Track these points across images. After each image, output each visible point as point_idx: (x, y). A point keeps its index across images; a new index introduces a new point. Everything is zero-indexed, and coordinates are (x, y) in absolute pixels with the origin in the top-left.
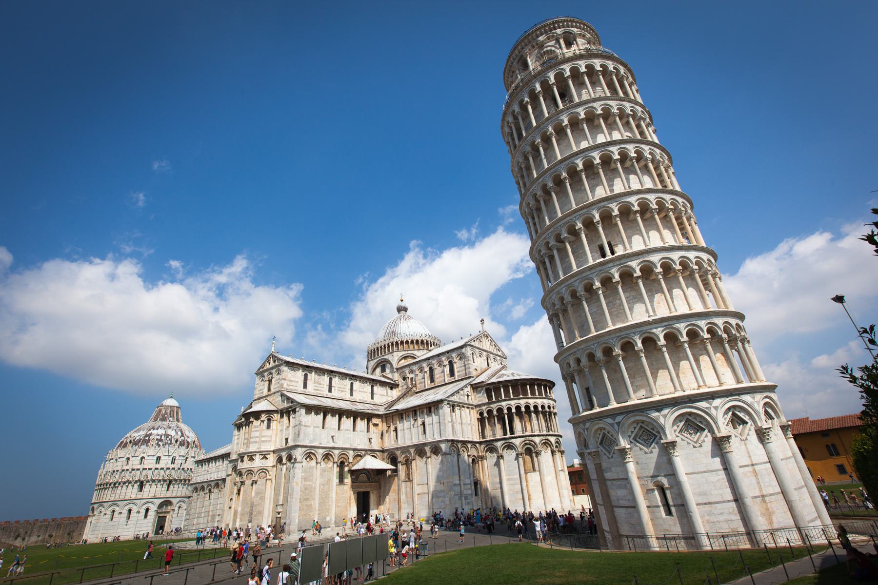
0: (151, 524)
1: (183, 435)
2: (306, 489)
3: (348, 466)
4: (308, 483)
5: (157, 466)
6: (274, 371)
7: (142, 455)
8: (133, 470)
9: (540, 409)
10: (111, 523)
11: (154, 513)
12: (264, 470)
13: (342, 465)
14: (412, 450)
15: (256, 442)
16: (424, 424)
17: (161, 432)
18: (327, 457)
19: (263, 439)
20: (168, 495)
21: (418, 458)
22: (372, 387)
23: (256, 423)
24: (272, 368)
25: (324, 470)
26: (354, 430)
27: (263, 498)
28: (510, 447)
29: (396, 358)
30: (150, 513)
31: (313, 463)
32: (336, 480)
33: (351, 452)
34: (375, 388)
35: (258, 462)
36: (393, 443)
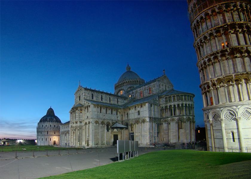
2: (96, 132)
13: (108, 126)
15: (77, 117)
16: (139, 112)
18: (103, 123)
21: (136, 123)
26: (112, 114)
28: (173, 120)
31: (98, 124)
32: (106, 130)
35: (79, 124)
36: (126, 119)
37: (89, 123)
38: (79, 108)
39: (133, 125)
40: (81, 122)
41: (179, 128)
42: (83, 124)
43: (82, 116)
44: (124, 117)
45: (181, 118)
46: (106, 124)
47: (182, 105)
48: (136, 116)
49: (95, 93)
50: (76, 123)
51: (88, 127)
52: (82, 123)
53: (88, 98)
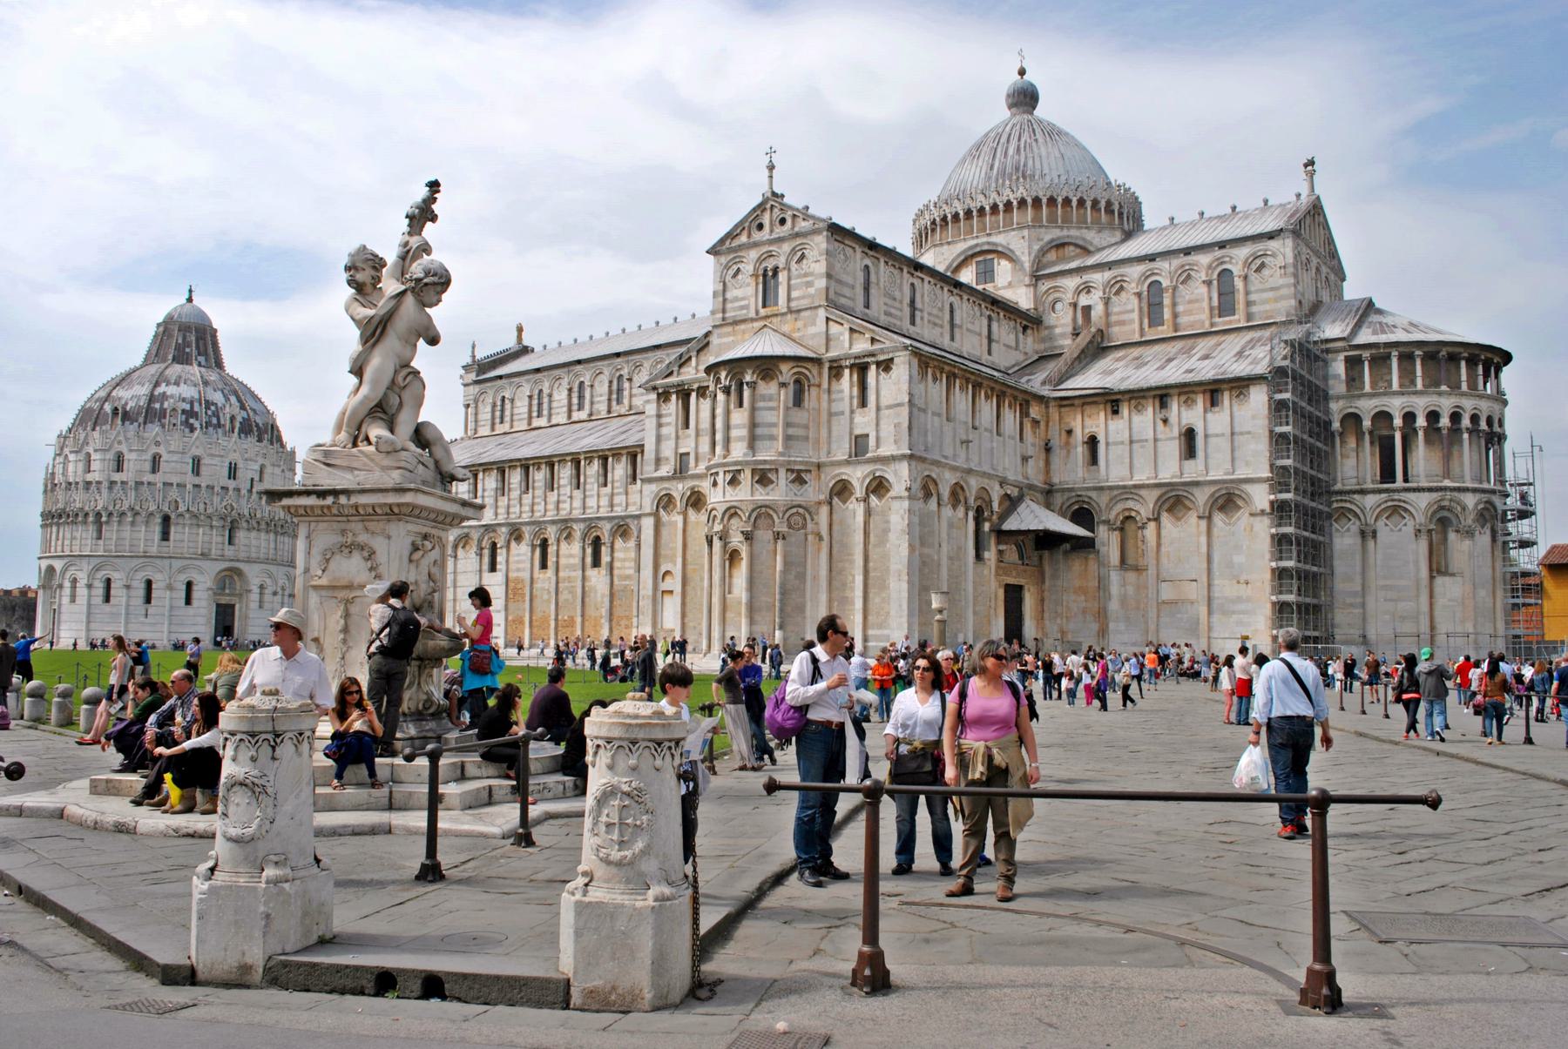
0: (201, 620)
1: (243, 407)
2: (924, 563)
3: (989, 520)
5: (197, 480)
6: (786, 247)
7: (154, 450)
8: (139, 484)
9: (1483, 425)
10: (107, 608)
11: (205, 595)
12: (799, 515)
14: (1151, 497)
15: (772, 438)
16: (1189, 435)
17: (188, 391)
19: (791, 431)
22: (990, 318)
23: (768, 388)
24: (780, 240)
25: (951, 525)
26: (998, 434)
27: (802, 577)
28: (1396, 511)
29: (1036, 247)
30: (196, 595)
32: (971, 552)
33: (997, 487)
34: (995, 325)
35: (780, 492)
37: (879, 486)
38: (784, 367)
39: (1143, 527)
41: (1438, 567)
42: (814, 492)
43: (806, 427)
44: (1056, 460)
45: (1446, 503)
47: (1455, 417)
48: (1171, 468)
50: (763, 477)
51: (860, 518)
52: (802, 482)
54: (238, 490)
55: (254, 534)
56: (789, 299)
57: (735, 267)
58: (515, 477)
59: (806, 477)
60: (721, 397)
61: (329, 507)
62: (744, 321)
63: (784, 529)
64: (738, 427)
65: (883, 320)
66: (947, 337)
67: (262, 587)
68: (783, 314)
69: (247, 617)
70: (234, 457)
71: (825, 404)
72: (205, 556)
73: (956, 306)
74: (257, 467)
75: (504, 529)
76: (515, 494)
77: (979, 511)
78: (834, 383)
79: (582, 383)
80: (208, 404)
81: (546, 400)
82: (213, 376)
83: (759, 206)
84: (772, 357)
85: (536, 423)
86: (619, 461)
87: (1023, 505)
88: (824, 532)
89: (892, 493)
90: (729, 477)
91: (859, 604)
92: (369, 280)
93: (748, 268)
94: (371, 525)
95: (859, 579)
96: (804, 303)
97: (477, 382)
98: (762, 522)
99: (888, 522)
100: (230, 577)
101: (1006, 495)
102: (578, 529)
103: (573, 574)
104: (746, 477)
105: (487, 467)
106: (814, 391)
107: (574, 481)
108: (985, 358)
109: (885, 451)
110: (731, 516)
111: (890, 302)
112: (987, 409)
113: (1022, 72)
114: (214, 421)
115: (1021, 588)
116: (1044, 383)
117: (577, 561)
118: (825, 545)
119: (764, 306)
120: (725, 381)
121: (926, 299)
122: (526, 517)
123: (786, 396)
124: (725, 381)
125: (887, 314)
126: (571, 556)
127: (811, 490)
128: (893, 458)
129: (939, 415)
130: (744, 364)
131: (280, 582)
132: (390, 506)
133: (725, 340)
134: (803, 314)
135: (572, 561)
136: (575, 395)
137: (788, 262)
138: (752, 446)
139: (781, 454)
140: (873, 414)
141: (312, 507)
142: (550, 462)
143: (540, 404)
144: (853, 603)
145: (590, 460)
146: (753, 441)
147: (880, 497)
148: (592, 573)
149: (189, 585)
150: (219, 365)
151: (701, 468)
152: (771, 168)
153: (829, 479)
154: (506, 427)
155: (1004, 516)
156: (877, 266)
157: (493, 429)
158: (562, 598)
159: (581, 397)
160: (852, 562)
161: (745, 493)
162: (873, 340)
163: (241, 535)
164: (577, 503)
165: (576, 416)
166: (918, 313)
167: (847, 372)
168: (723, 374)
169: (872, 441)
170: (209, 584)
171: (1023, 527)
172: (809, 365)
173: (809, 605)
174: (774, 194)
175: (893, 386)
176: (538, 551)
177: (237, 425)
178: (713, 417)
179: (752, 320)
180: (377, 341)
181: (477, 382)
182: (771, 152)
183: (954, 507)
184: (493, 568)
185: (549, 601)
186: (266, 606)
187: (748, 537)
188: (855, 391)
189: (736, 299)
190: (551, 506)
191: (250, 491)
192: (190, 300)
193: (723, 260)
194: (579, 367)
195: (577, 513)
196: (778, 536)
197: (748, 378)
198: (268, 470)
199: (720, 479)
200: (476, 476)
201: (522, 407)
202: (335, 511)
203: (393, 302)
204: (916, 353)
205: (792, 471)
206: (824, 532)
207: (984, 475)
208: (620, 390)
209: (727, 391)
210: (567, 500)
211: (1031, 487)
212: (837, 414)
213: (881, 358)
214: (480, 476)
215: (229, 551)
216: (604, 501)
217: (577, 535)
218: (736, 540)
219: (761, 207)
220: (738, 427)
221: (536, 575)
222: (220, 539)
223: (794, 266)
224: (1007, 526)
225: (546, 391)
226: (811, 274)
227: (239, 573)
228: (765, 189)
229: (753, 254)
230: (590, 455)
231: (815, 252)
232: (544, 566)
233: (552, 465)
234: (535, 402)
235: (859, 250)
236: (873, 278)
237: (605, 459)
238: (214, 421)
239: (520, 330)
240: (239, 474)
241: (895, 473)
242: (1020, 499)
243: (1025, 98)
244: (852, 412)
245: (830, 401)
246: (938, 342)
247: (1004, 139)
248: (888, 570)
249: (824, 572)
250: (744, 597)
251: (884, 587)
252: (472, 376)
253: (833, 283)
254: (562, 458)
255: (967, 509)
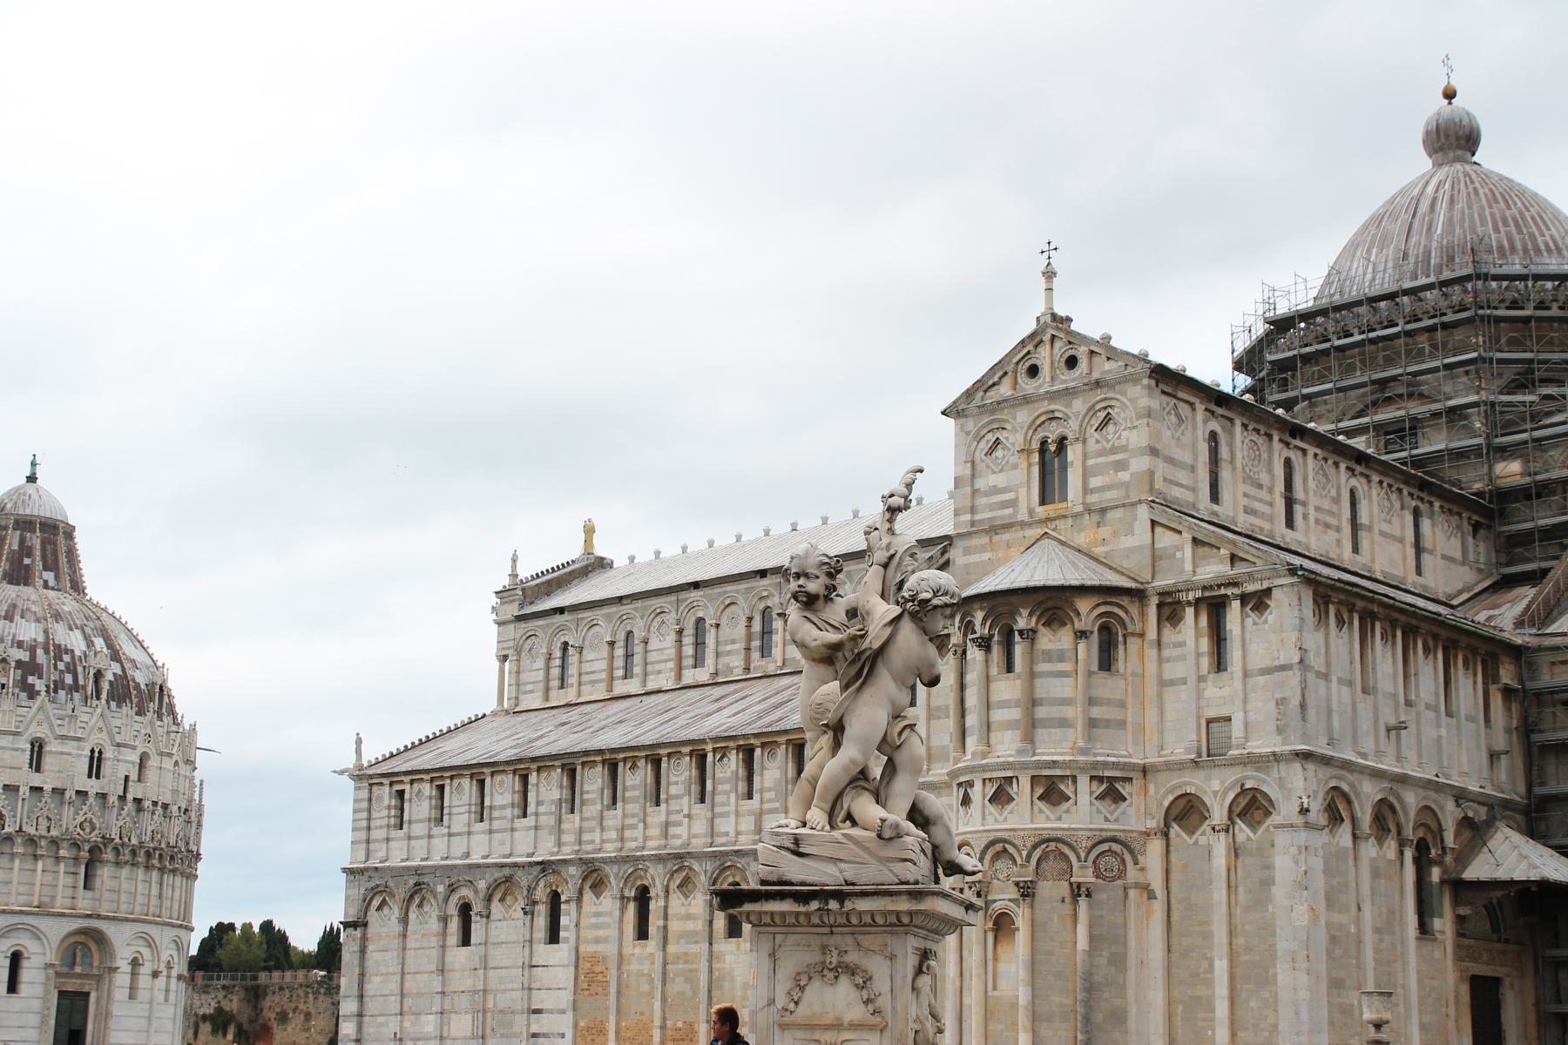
0: (33, 1020)
1: (116, 656)
2: (1333, 940)
3: (1440, 863)
4: (1338, 918)
5: (36, 779)
6: (1079, 405)
12: (1114, 851)
15: (1064, 723)
17: (29, 631)
19: (1096, 712)
20: (85, 902)
22: (1417, 513)
23: (1055, 640)
24: (1069, 393)
25: (1375, 873)
27: (1119, 961)
31: (1344, 835)
33: (1450, 805)
34: (1426, 524)
35: (1082, 815)
37: (1252, 806)
38: (1084, 605)
40: (1112, 794)
42: (1139, 813)
43: (1122, 705)
46: (1409, 832)
49: (1238, 428)
50: (1051, 791)
53: (1176, 492)
54: (103, 796)
55: (125, 871)
56: (1086, 490)
57: (991, 438)
58: (593, 781)
59: (1124, 789)
60: (975, 654)
61: (808, 915)
62: (1007, 527)
63: (1085, 876)
64: (1004, 704)
65: (1243, 522)
66: (1348, 546)
67: (135, 963)
68: (1076, 516)
69: (108, 1014)
70: (98, 739)
71: (1151, 667)
72: (43, 910)
73: (1360, 493)
74: (134, 757)
75: (572, 870)
76: (592, 810)
77: (1422, 848)
78: (1169, 634)
79: (700, 621)
80: (60, 651)
81: (638, 649)
82: (68, 604)
83: (1032, 336)
84: (1062, 588)
85: (620, 688)
86: (772, 754)
87: (1499, 836)
88: (1157, 885)
89: (1275, 819)
90: (990, 791)
91: (1222, 1010)
92: (822, 592)
93: (1014, 438)
94: (866, 941)
95: (1221, 966)
96: (1111, 495)
97: (520, 618)
98: (1050, 866)
99: (1269, 867)
100: (88, 944)
101: (1466, 818)
102: (703, 873)
103: (694, 948)
104: (1022, 791)
105: (543, 763)
106: (1133, 644)
107: (695, 789)
108: (1412, 580)
109: (1263, 745)
110: (997, 856)
111: (1253, 491)
112: (1428, 672)
113: (1450, 95)
114: (69, 679)
115: (1496, 981)
116: (1519, 624)
117: (699, 925)
118: (1158, 907)
119: (1043, 502)
120: (981, 630)
121: (1312, 484)
122: (610, 850)
123: (1087, 652)
124: (981, 630)
125: (1248, 511)
126: (689, 917)
127: (1132, 811)
128: (1276, 757)
129: (1350, 684)
130: (1014, 599)
131: (165, 956)
132: (898, 914)
133: (975, 558)
134: (1110, 515)
135: (691, 926)
136: (688, 640)
137: (1082, 429)
138: (1029, 738)
139: (1084, 751)
140: (1238, 683)
141: (783, 914)
142: (654, 757)
143: (628, 656)
144: (1211, 1009)
145: (723, 753)
146: (1030, 727)
147: (1254, 825)
148: (726, 947)
149: (16, 959)
150: (77, 587)
151: (939, 772)
152: (1049, 274)
153: (1161, 793)
154: (570, 695)
155: (1464, 858)
156: (1231, 433)
157: (547, 699)
158: (672, 990)
159: (699, 644)
160: (1207, 936)
161: (1025, 817)
162: (1234, 558)
163: (105, 874)
164: (700, 827)
165: (689, 676)
166: (1298, 509)
167: (1190, 611)
168: (979, 616)
169: (1237, 729)
170: (51, 957)
171: (1502, 874)
172: (1125, 601)
173: (1133, 1011)
174: (1054, 316)
175: (1276, 635)
176: (632, 907)
177: (105, 686)
178: (962, 687)
179: (1023, 525)
180: (864, 683)
181: (520, 618)
182: (1050, 249)
183: (1380, 841)
184: (554, 936)
185: (651, 994)
186: (143, 994)
187: (1026, 892)
188: (1205, 644)
189: (995, 490)
190: (655, 832)
191: (122, 798)
192: (32, 479)
193: (970, 425)
194: (695, 595)
195: (698, 844)
196: (1077, 891)
197: (1022, 623)
198: (153, 762)
199: (976, 793)
200: (525, 779)
201: (595, 660)
202: (815, 920)
203: (889, 631)
204: (1311, 580)
205: (1100, 779)
206: (1157, 885)
207: (1429, 784)
208: (766, 633)
209: (985, 644)
210: (685, 822)
211: (1506, 805)
212: (1172, 683)
213: (1250, 588)
214: (533, 778)
215: (85, 902)
216: (747, 824)
217: (702, 881)
218: (1003, 896)
219: (1034, 339)
220: (1004, 704)
221: (627, 950)
222: (70, 880)
223: (1092, 436)
224: (1470, 874)
225: (638, 635)
226: (1124, 449)
227: (99, 938)
228: (1040, 309)
229: (1023, 416)
230: (723, 743)
231: (1130, 413)
232: (642, 934)
233: (657, 763)
234: (619, 652)
235: (1200, 407)
236: (1224, 452)
237: (748, 753)
238: (69, 679)
239: (589, 531)
240: (107, 768)
241: (1281, 782)
242: (1489, 824)
243: (1454, 140)
244: (1201, 679)
245: (1160, 661)
246: (1333, 556)
247: (1424, 207)
248: (1272, 952)
249: (1157, 952)
250: (1023, 995)
251: (1265, 979)
252: (513, 610)
253: (1161, 468)
254: (675, 748)
255: (1402, 844)
